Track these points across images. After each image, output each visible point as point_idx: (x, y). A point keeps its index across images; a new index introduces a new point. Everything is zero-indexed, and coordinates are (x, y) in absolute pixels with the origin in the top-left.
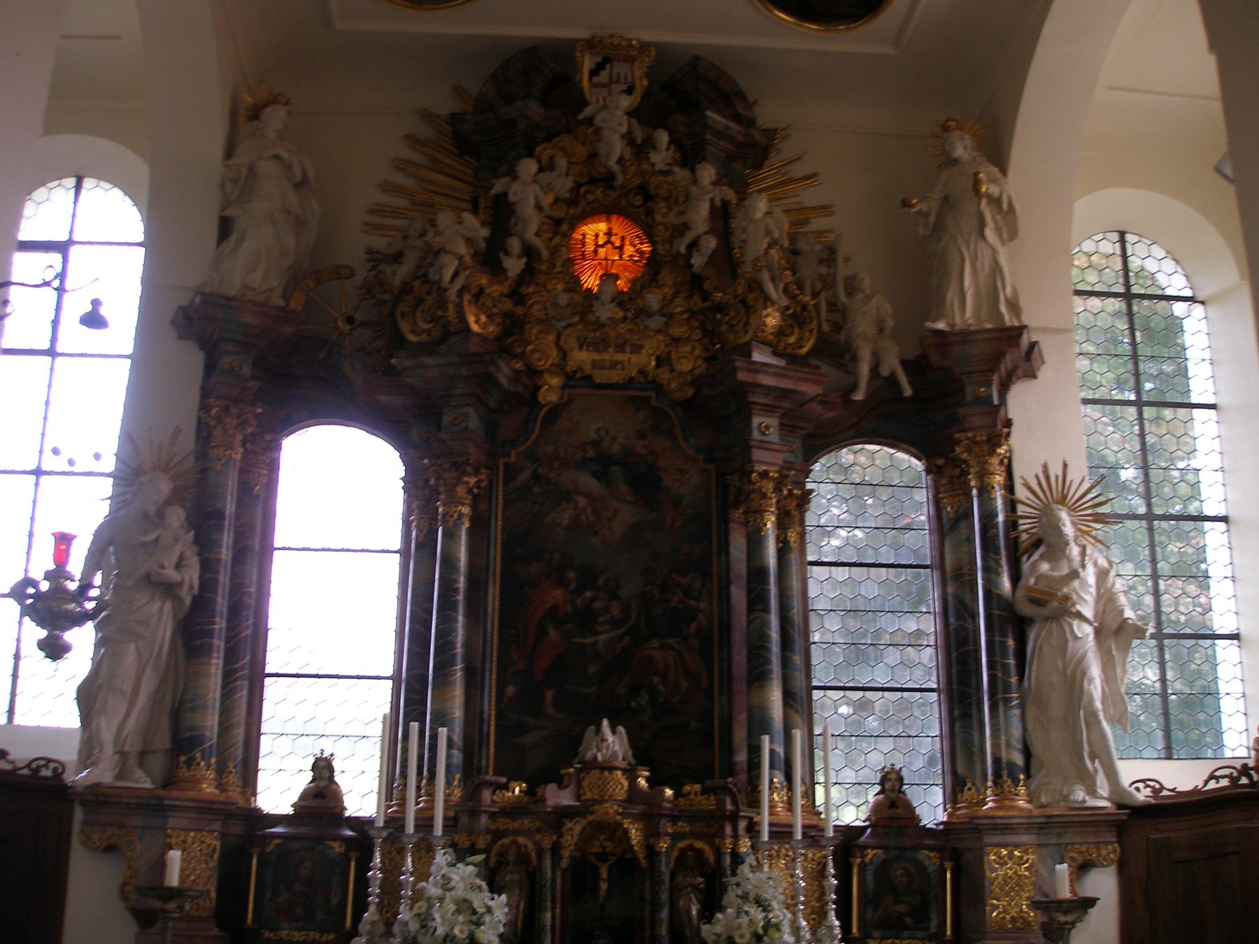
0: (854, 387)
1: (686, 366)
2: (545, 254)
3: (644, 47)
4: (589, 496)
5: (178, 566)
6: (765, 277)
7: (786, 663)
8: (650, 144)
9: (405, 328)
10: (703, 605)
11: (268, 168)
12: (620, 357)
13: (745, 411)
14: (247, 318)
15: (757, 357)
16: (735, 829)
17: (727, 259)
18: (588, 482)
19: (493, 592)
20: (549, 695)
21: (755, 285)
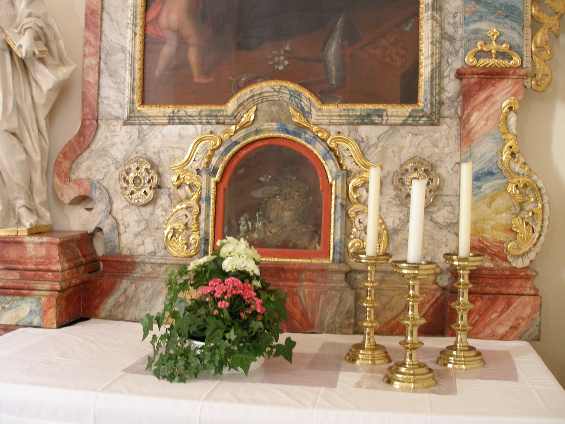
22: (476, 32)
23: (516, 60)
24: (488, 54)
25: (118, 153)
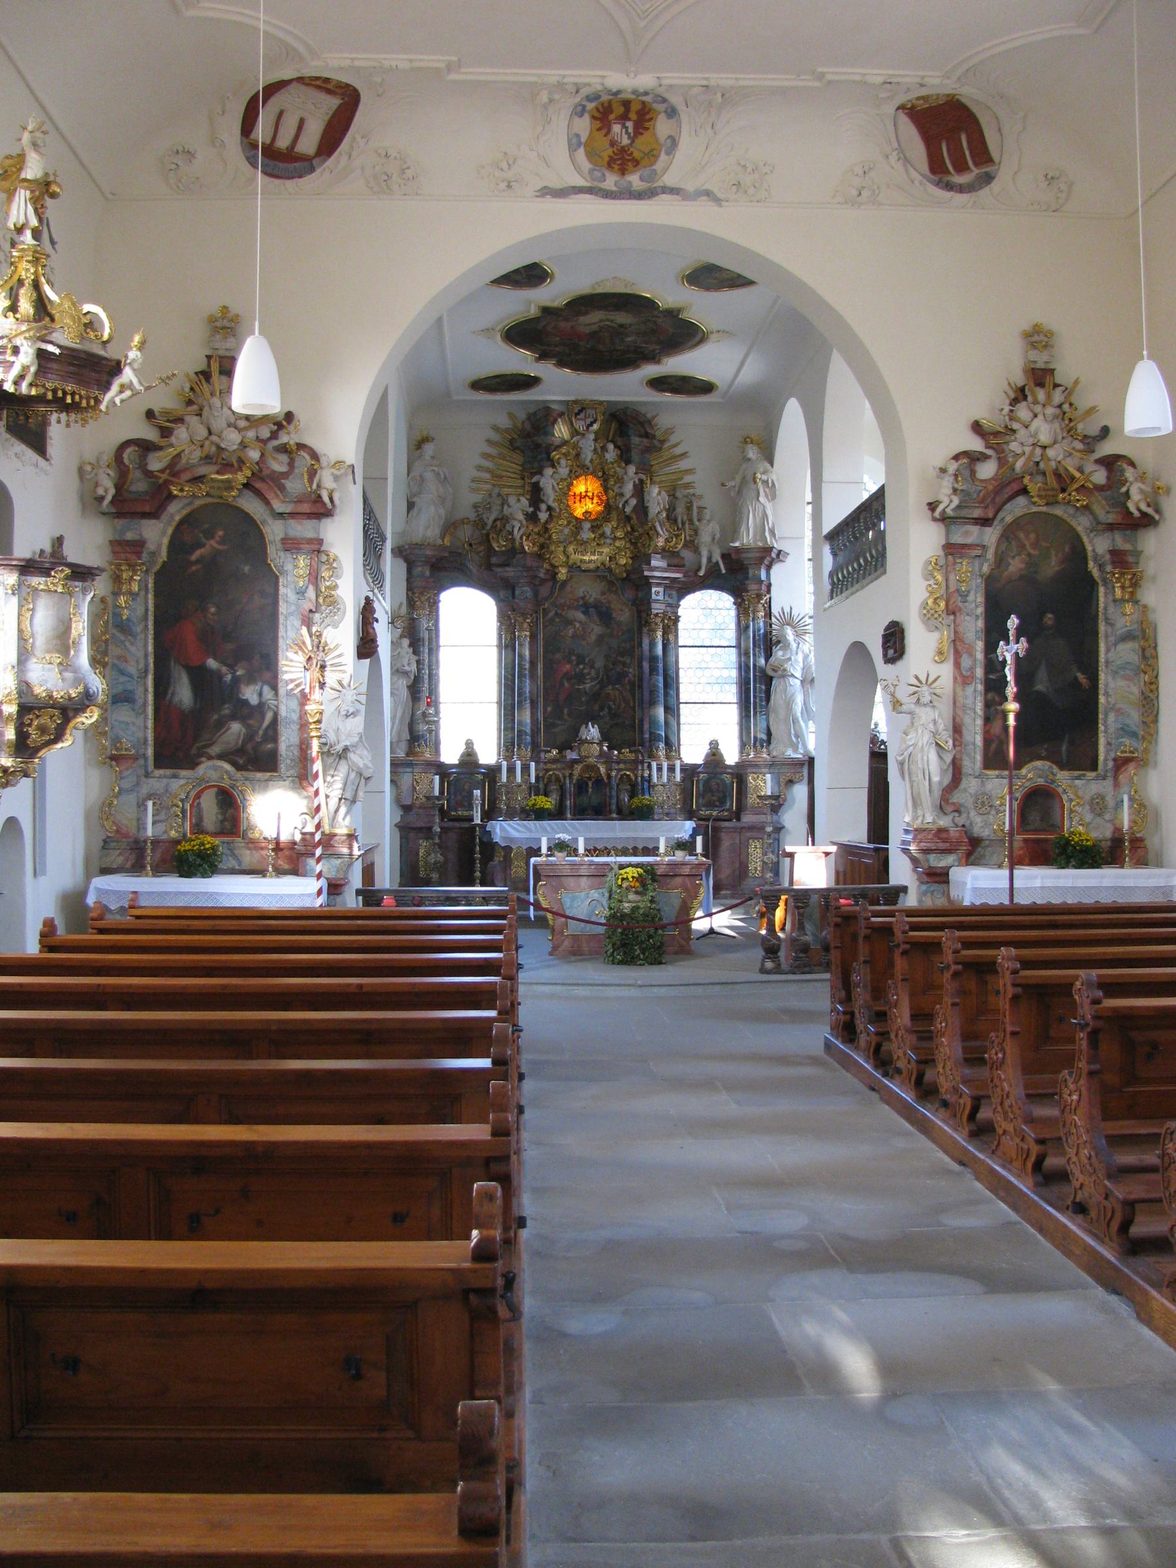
0: (699, 569)
1: (623, 561)
2: (558, 510)
3: (601, 403)
4: (580, 622)
5: (409, 664)
6: (657, 524)
7: (666, 694)
8: (604, 448)
9: (495, 545)
10: (631, 670)
11: (429, 475)
12: (593, 558)
13: (649, 586)
14: (428, 552)
15: (654, 563)
16: (643, 767)
17: (642, 509)
18: (580, 616)
19: (540, 666)
20: (566, 711)
21: (654, 528)
22: (1121, 742)
23: (1136, 755)
24: (1125, 752)
25: (972, 790)
